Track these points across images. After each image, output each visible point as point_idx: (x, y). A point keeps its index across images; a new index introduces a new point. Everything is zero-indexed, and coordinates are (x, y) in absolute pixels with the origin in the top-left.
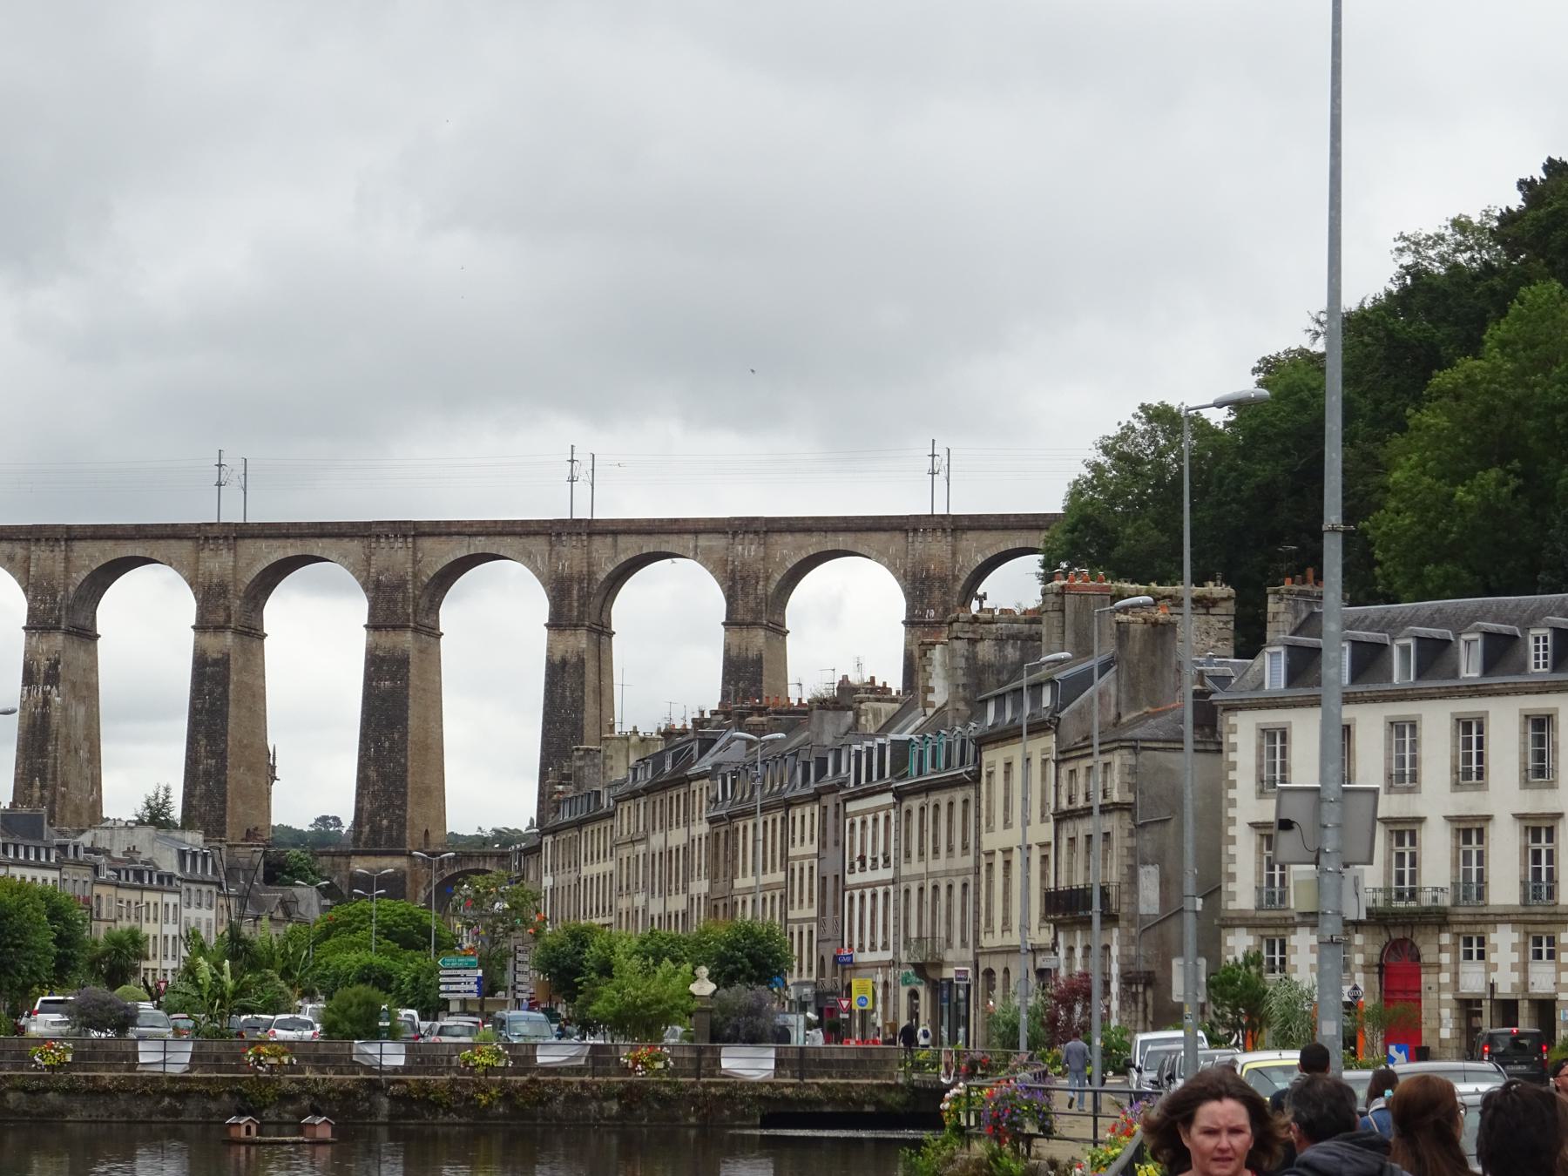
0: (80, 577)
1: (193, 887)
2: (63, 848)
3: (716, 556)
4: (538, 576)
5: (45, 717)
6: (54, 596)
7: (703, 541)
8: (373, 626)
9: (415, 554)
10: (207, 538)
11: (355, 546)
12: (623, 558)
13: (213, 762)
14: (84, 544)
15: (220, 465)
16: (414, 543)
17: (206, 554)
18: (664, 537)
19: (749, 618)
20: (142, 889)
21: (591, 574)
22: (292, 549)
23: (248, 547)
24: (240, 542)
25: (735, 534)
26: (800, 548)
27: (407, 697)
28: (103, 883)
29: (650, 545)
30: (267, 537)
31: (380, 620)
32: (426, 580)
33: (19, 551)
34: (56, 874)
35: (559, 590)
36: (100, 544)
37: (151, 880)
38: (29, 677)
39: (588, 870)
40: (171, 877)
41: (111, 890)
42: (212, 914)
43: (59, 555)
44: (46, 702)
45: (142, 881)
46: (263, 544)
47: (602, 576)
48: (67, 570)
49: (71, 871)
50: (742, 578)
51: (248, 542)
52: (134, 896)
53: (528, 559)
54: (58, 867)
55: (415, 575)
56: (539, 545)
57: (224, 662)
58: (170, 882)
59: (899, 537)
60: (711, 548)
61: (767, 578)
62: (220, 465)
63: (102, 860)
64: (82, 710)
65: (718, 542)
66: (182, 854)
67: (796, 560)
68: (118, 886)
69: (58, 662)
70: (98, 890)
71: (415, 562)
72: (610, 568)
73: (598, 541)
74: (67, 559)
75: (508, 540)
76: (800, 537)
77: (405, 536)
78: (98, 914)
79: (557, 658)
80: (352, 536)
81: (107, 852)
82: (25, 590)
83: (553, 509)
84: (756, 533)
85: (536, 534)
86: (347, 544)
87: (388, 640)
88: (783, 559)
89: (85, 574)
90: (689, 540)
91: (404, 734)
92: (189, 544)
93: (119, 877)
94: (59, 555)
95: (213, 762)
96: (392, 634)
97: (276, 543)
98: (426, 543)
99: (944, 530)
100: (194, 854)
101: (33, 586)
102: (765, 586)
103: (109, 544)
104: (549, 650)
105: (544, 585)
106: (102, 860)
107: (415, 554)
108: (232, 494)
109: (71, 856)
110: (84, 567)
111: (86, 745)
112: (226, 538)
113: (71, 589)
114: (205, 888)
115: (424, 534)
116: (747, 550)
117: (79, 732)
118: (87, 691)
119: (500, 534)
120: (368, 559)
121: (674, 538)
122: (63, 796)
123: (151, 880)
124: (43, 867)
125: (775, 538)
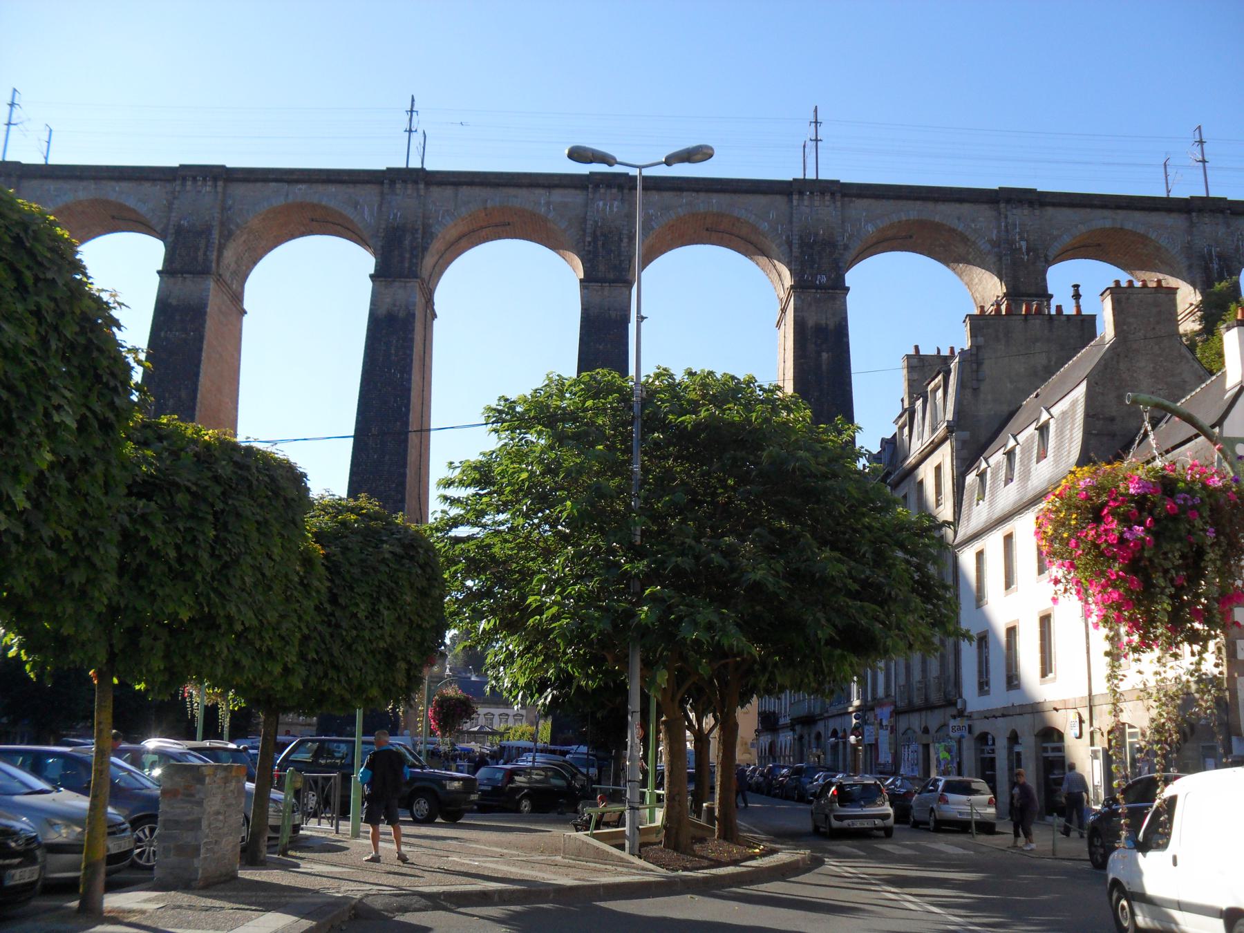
7: (557, 196)
16: (225, 188)
18: (512, 191)
19: (611, 276)
25: (597, 186)
27: (200, 350)
50: (603, 235)
59: (780, 200)
71: (224, 209)
73: (436, 191)
75: (332, 189)
76: (667, 196)
79: (382, 311)
87: (187, 288)
91: (195, 391)
98: (239, 190)
99: (833, 194)
104: (374, 303)
120: (170, 204)
121: (523, 193)
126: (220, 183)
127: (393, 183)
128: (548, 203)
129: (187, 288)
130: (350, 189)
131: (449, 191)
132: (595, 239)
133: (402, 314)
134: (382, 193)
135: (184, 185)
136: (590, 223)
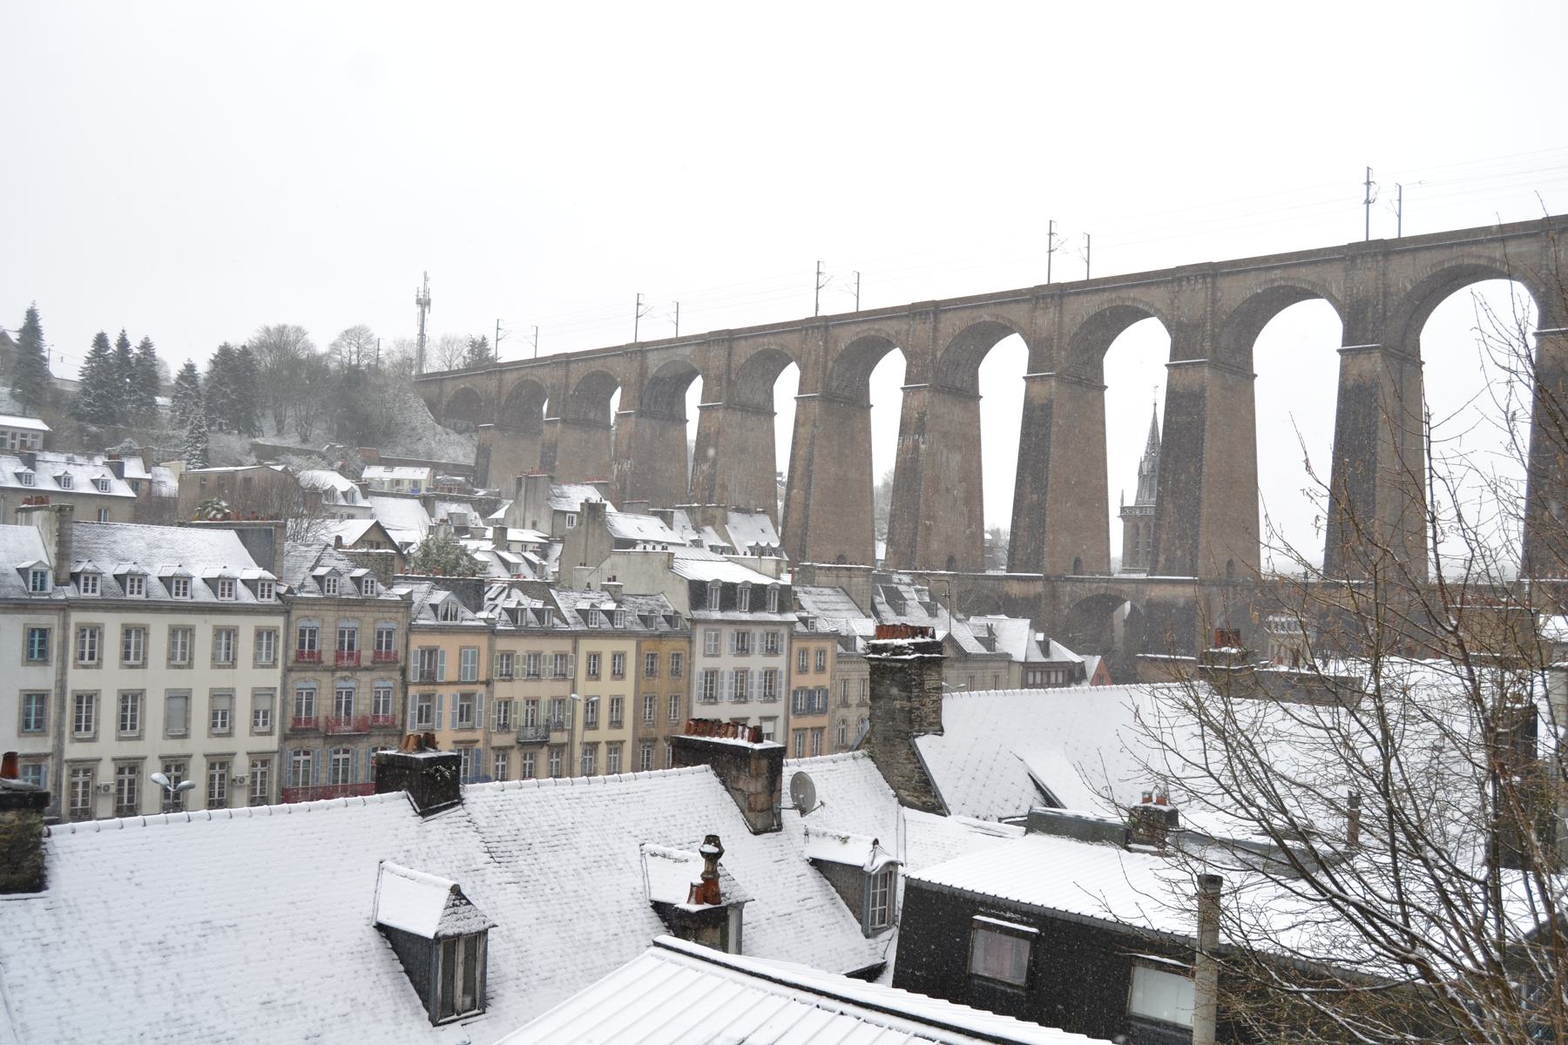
5: (915, 461)
13: (1035, 497)
16: (1214, 284)
17: (1038, 313)
38: (903, 431)
44: (916, 448)
55: (1213, 313)
57: (1047, 408)
64: (956, 459)
69: (924, 414)
71: (1214, 301)
74: (935, 329)
77: (1204, 277)
79: (1350, 383)
83: (1347, 233)
92: (1025, 307)
94: (929, 326)
95: (1035, 497)
98: (1224, 283)
122: (929, 528)
127: (1353, 259)
129: (1192, 379)
131: (1408, 258)
134: (1346, 270)
135: (1180, 286)
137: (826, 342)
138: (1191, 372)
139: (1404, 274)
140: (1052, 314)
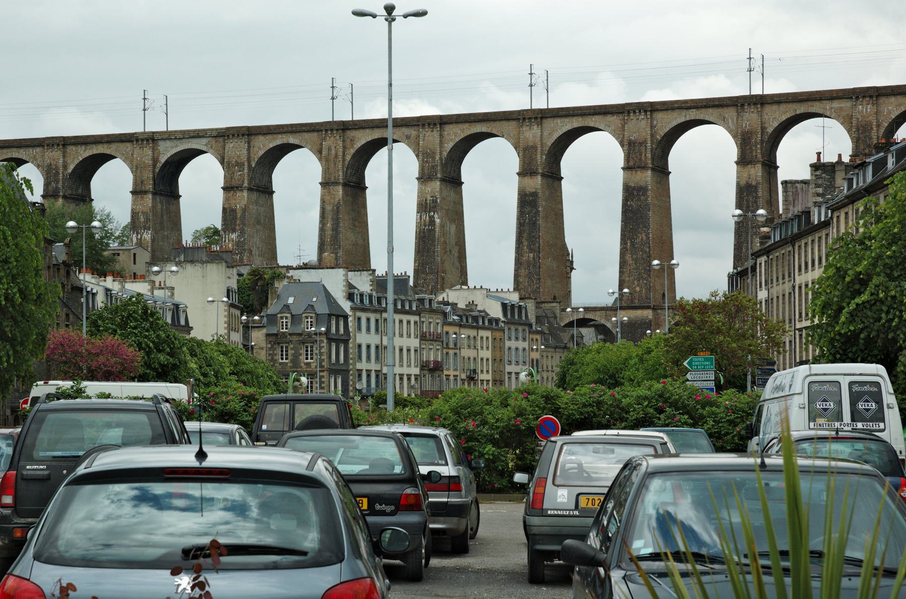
0: (449, 146)
1: (513, 328)
2: (421, 301)
3: (844, 113)
4: (730, 132)
6: (434, 158)
7: (836, 104)
8: (628, 168)
9: (652, 122)
10: (524, 119)
11: (615, 120)
12: (784, 118)
13: (531, 255)
14: (451, 126)
15: (531, 74)
16: (651, 115)
17: (525, 128)
18: (810, 103)
20: (478, 328)
21: (763, 129)
22: (576, 123)
23: (549, 124)
24: (544, 121)
25: (857, 98)
26: (900, 105)
28: (450, 324)
29: (801, 109)
30: (561, 116)
31: (631, 163)
32: (659, 137)
33: (413, 132)
34: (417, 318)
35: (744, 141)
36: (460, 126)
37: (483, 322)
39: (800, 279)
40: (497, 321)
41: (456, 329)
42: (526, 345)
43: (436, 134)
44: (432, 222)
45: (477, 322)
46: (559, 121)
47: (770, 130)
48: (441, 143)
49: (427, 316)
51: (550, 120)
52: (472, 333)
53: (723, 122)
54: (418, 313)
55: (652, 135)
56: (731, 113)
58: (497, 324)
60: (841, 108)
61: (878, 126)
62: (531, 74)
63: (448, 309)
64: (453, 228)
65: (846, 104)
66: (504, 306)
67: (897, 113)
68: (460, 326)
70: (446, 328)
71: (652, 127)
72: (776, 124)
74: (441, 136)
75: (710, 110)
78: (447, 344)
79: (743, 183)
80: (612, 113)
81: (454, 305)
82: (417, 156)
84: (871, 97)
85: (727, 106)
86: (610, 118)
88: (889, 113)
89: (451, 145)
90: (827, 106)
92: (514, 123)
93: (461, 320)
94: (436, 134)
95: (531, 255)
96: (639, 173)
97: (566, 120)
98: (659, 116)
100: (513, 306)
101: (423, 155)
102: (878, 130)
103: (467, 125)
104: (738, 177)
105: (734, 137)
106: (449, 309)
107: (652, 122)
108: (539, 90)
109: (427, 307)
110: (452, 140)
111: (456, 249)
112: (536, 118)
113: (445, 154)
114: (520, 328)
115: (657, 110)
116: (865, 109)
117: (453, 240)
118: (457, 215)
119: (706, 107)
120: (623, 126)
121: (817, 104)
123: (483, 322)
124: (410, 312)
125: (882, 100)
126: (649, 113)
127: (743, 105)
128: (831, 108)
130: (720, 110)
131: (775, 107)
132: (858, 129)
133: (754, 183)
136: (854, 122)
137: (344, 141)
138: (639, 173)
139: (774, 117)
140: (536, 130)
